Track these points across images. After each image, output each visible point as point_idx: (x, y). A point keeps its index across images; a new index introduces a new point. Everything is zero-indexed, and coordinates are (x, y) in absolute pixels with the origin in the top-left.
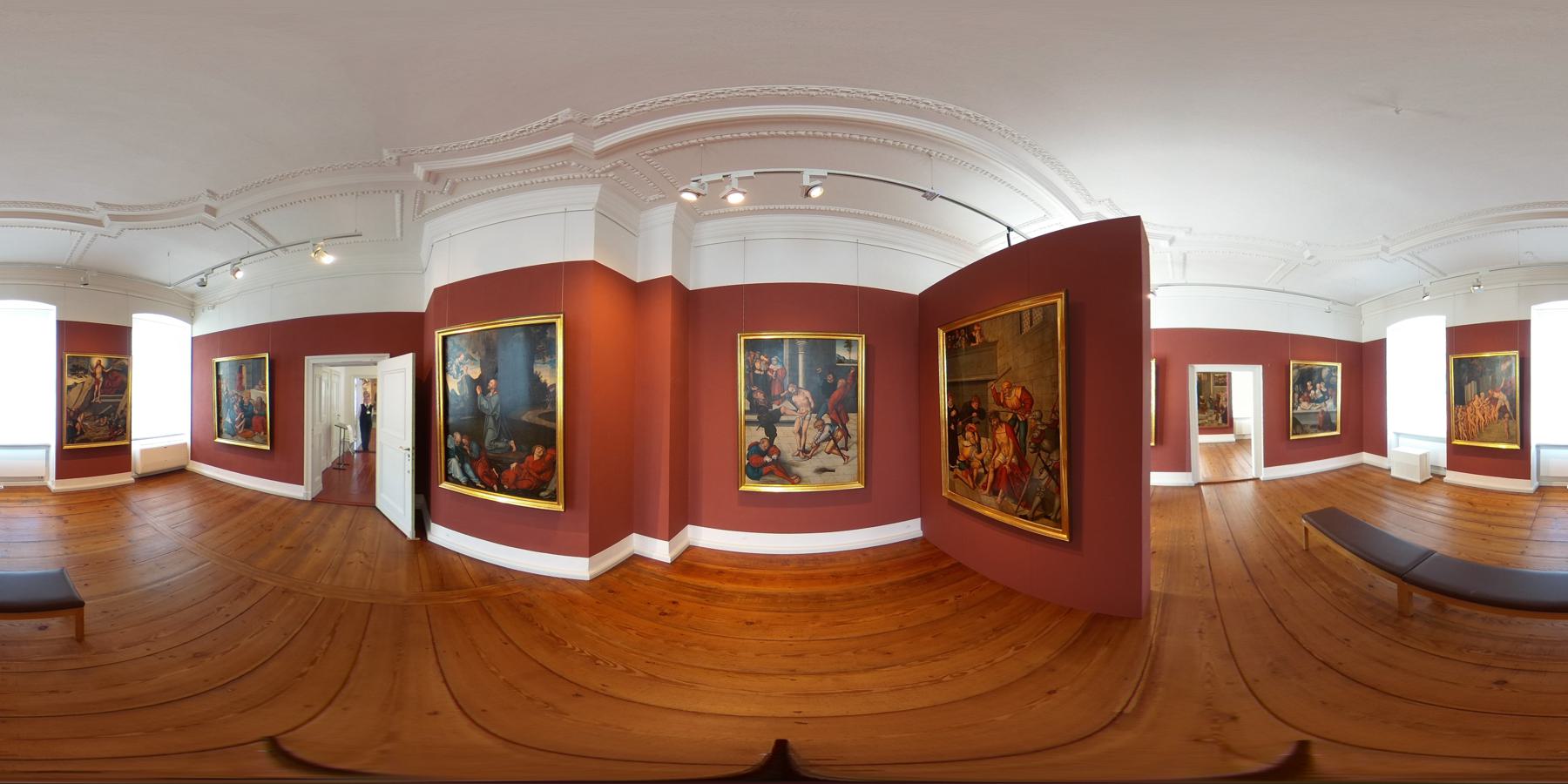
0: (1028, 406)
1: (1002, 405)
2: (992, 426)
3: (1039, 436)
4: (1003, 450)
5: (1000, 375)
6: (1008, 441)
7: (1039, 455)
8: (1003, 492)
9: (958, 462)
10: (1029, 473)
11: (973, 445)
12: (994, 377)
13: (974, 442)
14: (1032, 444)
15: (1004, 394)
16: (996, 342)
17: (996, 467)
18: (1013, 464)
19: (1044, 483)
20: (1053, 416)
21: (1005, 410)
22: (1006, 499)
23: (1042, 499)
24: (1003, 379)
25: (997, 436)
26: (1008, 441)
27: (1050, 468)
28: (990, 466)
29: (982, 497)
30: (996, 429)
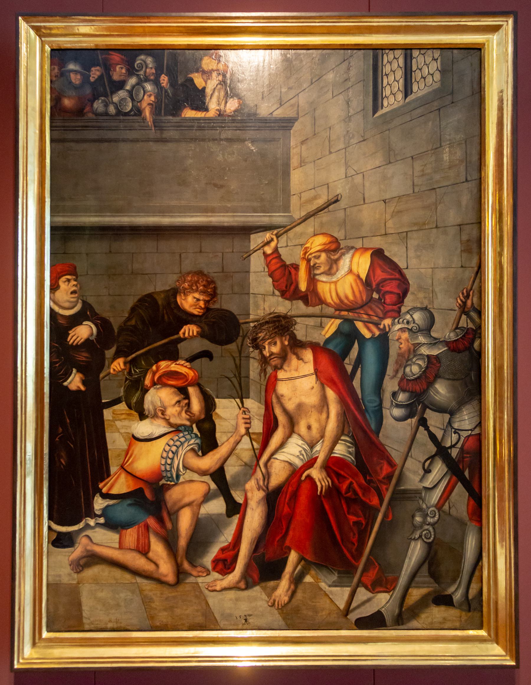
0: (389, 299)
1: (305, 298)
2: (264, 361)
3: (425, 372)
4: (302, 428)
5: (297, 214)
6: (324, 400)
7: (423, 422)
8: (301, 559)
9: (99, 504)
10: (389, 477)
11: (177, 429)
12: (278, 218)
13: (183, 420)
14: (402, 397)
15: (311, 269)
16: (295, 119)
17: (275, 481)
18: (340, 462)
19: (435, 496)
20: (464, 322)
21: (310, 310)
22: (308, 579)
23: (430, 545)
24: (309, 227)
25: (283, 388)
26: (324, 400)
27: (454, 453)
28: (251, 485)
29: (213, 600)
30: (277, 368)
